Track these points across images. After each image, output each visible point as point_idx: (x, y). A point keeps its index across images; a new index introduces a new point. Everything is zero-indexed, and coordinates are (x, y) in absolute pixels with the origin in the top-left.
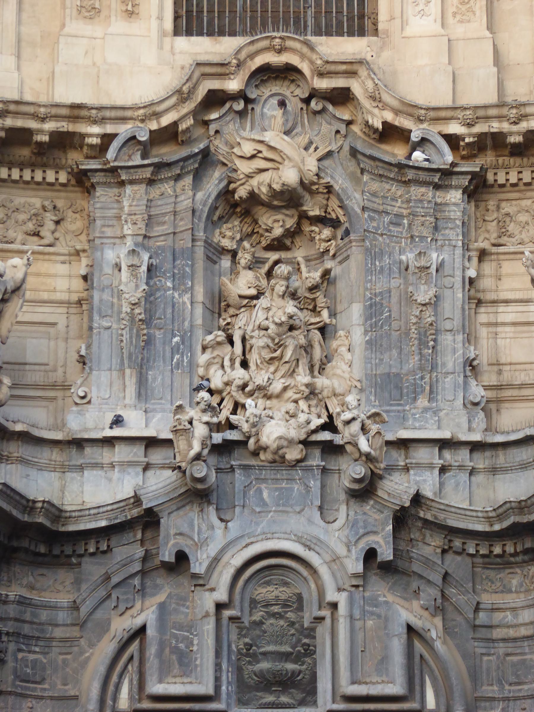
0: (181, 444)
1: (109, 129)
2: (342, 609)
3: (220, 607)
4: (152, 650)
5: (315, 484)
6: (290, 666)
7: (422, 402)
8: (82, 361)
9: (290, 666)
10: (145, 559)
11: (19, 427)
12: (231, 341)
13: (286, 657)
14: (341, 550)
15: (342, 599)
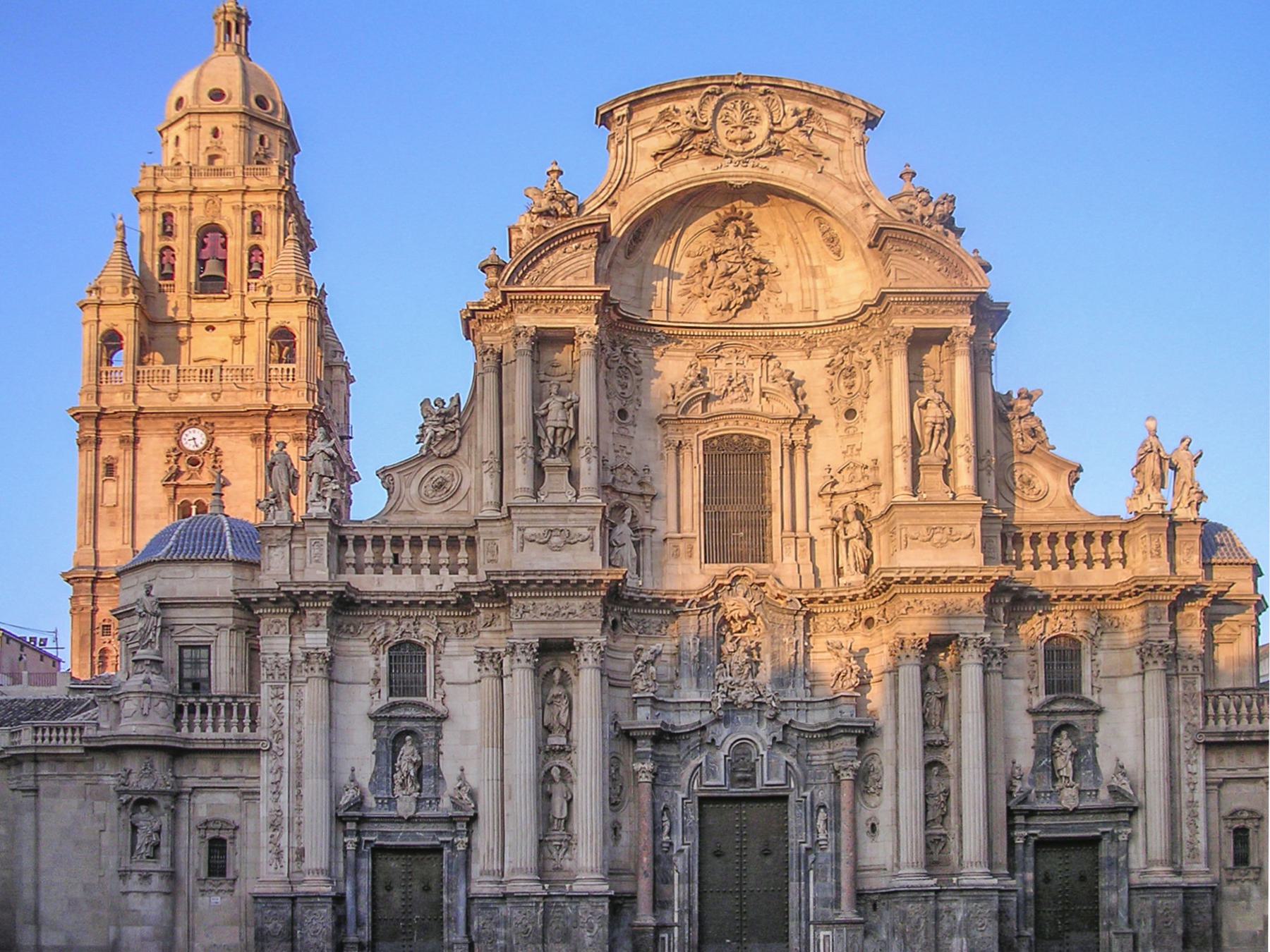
0: (714, 704)
1: (686, 597)
2: (765, 757)
3: (725, 756)
4: (704, 772)
5: (756, 715)
6: (748, 775)
7: (791, 687)
8: (677, 675)
9: (748, 775)
10: (701, 741)
11: (661, 699)
12: (725, 666)
13: (746, 772)
14: (764, 737)
15: (765, 753)
